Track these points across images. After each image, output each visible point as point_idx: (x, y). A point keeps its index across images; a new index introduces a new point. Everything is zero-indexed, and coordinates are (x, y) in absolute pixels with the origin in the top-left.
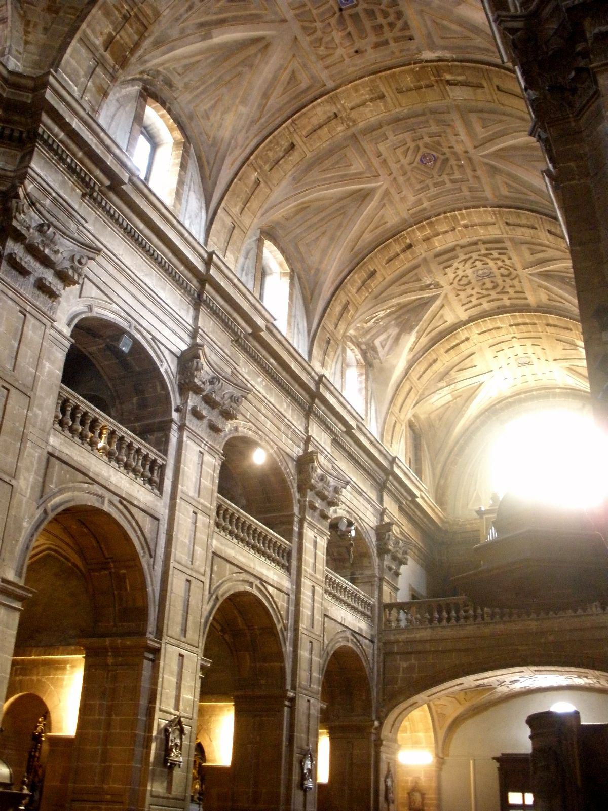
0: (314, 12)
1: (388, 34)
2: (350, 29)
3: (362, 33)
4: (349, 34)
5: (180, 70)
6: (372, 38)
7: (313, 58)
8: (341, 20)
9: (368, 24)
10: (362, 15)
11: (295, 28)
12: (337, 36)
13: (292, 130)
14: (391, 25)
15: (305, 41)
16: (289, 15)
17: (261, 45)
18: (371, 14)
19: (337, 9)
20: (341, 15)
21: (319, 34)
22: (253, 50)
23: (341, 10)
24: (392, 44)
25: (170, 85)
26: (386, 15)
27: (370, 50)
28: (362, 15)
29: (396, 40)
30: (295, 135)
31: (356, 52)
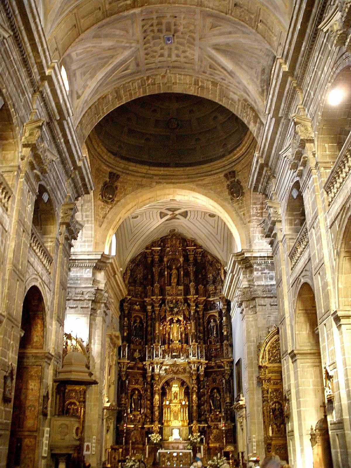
0: (186, 42)
1: (155, 22)
2: (173, 28)
3: (168, 24)
4: (175, 25)
5: (254, 70)
6: (164, 21)
7: (197, 27)
8: (176, 31)
9: (164, 27)
10: (164, 31)
11: (197, 42)
12: (181, 29)
13: (230, 12)
14: (152, 25)
15: (197, 36)
16: (196, 48)
17: (217, 47)
18: (160, 31)
19: (175, 37)
20: (175, 33)
21: (189, 34)
22: (222, 47)
23: (174, 36)
24: (155, 17)
25: (263, 70)
26: (153, 31)
27: (168, 15)
28: (164, 31)
29: (153, 19)
30: (230, 8)
31: (176, 17)
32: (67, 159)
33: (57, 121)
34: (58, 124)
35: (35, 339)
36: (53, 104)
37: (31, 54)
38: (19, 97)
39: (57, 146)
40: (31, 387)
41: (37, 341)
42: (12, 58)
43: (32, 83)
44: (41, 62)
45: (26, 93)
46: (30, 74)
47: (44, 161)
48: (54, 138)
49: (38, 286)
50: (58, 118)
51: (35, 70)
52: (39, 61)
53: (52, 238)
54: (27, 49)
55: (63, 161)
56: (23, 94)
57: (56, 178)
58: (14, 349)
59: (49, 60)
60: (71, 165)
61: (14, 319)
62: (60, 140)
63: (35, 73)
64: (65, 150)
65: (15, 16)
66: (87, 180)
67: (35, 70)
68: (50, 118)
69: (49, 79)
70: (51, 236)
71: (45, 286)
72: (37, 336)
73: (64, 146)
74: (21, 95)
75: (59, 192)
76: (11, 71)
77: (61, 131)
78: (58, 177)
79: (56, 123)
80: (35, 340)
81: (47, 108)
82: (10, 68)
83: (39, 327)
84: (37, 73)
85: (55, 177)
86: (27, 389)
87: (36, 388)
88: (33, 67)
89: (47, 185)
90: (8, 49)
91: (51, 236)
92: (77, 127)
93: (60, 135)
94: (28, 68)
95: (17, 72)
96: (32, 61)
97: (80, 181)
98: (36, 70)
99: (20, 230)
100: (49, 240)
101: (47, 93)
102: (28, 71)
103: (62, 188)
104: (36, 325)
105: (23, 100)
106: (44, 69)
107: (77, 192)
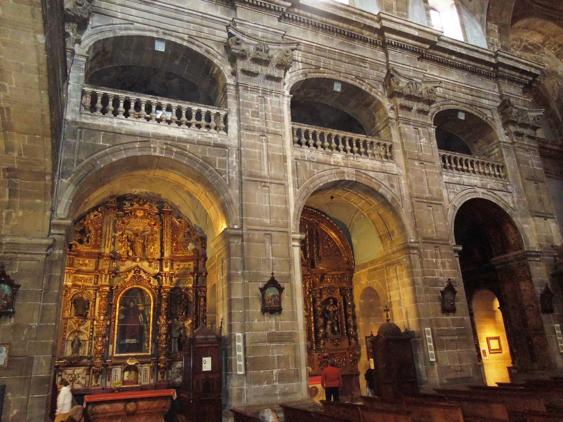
32: (476, 67)
33: (430, 48)
34: (434, 50)
35: (512, 242)
36: (410, 41)
37: (351, 27)
38: (361, 66)
39: (453, 66)
40: (522, 288)
41: (514, 244)
42: (328, 48)
43: (374, 44)
44: (365, 25)
45: (367, 59)
46: (364, 40)
47: (420, 96)
48: (441, 63)
49: (481, 196)
50: (428, 46)
51: (366, 33)
52: (362, 25)
53: (495, 144)
54: (343, 27)
55: (473, 72)
56: (364, 61)
57: (468, 91)
58: (447, 264)
59: (372, 16)
60: (487, 68)
61: (435, 240)
62: (451, 59)
63: (369, 35)
64: (465, 61)
65: (311, 18)
66: (521, 67)
67: (366, 33)
68: (419, 53)
69: (384, 29)
70: (495, 142)
71: (496, 192)
72: (513, 239)
73: (461, 60)
74: (361, 64)
75: (484, 101)
76: (336, 57)
77: (446, 53)
78: (471, 90)
79: (431, 51)
80: (512, 243)
81: (407, 49)
82: (333, 56)
83: (511, 230)
84: (371, 34)
85: (468, 91)
86: (520, 290)
87: (527, 288)
88: (362, 34)
89: (457, 105)
90: (319, 46)
91: (495, 142)
92: (487, 24)
93: (447, 55)
94: (358, 38)
95: (343, 52)
96: (357, 30)
97: (514, 73)
98: (367, 33)
99: (415, 166)
100: (495, 146)
101: (395, 39)
102: (361, 39)
103: (489, 94)
104: (508, 229)
105: (367, 65)
106: (373, 27)
107: (519, 83)
